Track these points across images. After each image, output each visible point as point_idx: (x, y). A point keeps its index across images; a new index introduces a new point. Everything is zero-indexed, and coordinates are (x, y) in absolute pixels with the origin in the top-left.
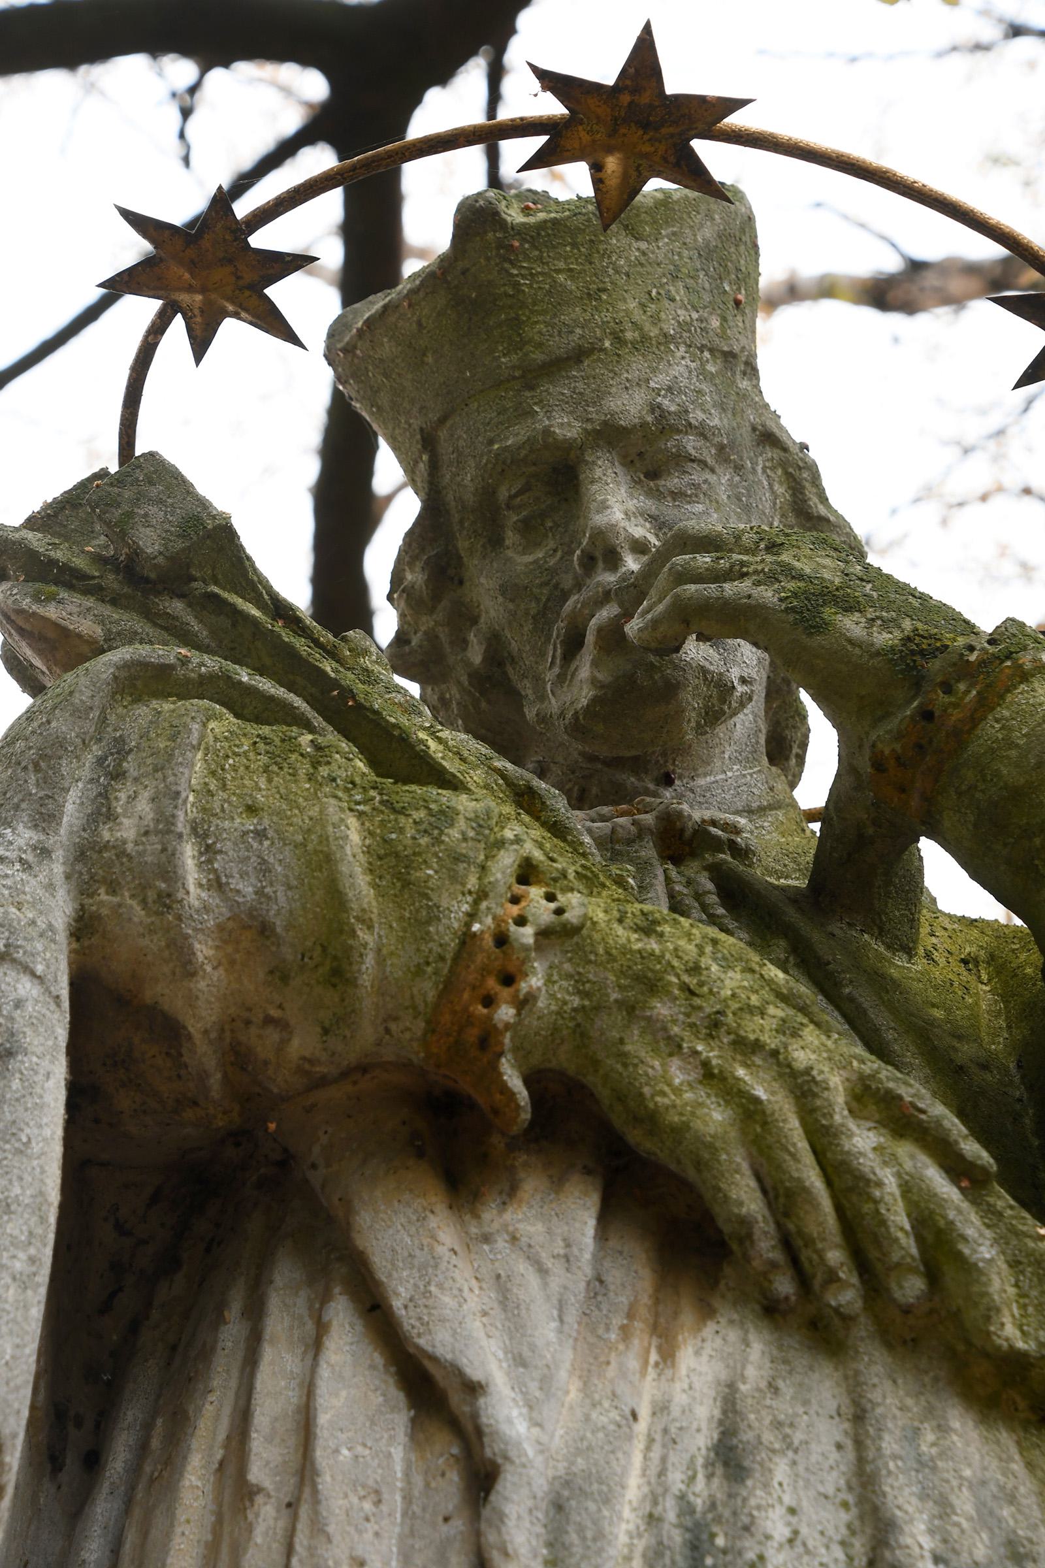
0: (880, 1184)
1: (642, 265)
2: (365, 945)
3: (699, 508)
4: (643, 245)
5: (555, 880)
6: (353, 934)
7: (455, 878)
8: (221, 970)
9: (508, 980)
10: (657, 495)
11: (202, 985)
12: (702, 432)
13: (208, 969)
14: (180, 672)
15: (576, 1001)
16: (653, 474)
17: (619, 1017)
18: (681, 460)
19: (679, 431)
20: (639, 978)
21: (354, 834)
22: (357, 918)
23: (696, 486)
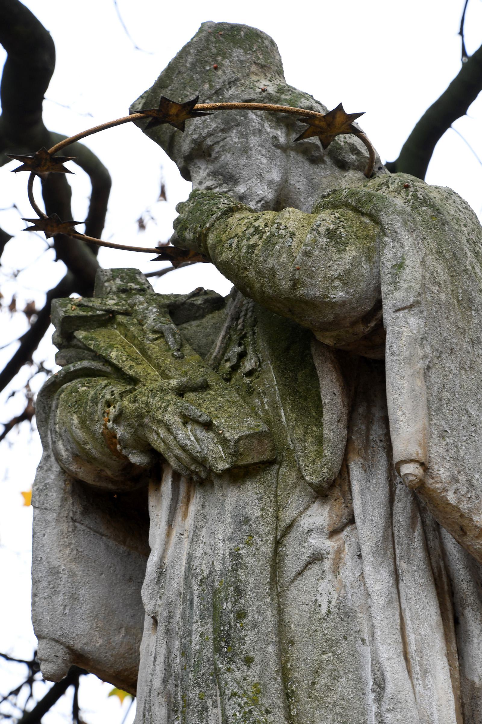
0: (186, 445)
1: (172, 94)
2: (90, 449)
3: (223, 157)
4: (170, 88)
5: (114, 402)
6: (85, 449)
7: (92, 420)
8: (83, 468)
9: (115, 437)
10: (213, 162)
11: (81, 474)
12: (210, 134)
13: (79, 470)
14: (58, 380)
15: (133, 430)
16: (210, 155)
17: (141, 429)
18: (210, 148)
19: (203, 141)
20: (138, 416)
21: (76, 421)
22: (83, 444)
23: (218, 152)
